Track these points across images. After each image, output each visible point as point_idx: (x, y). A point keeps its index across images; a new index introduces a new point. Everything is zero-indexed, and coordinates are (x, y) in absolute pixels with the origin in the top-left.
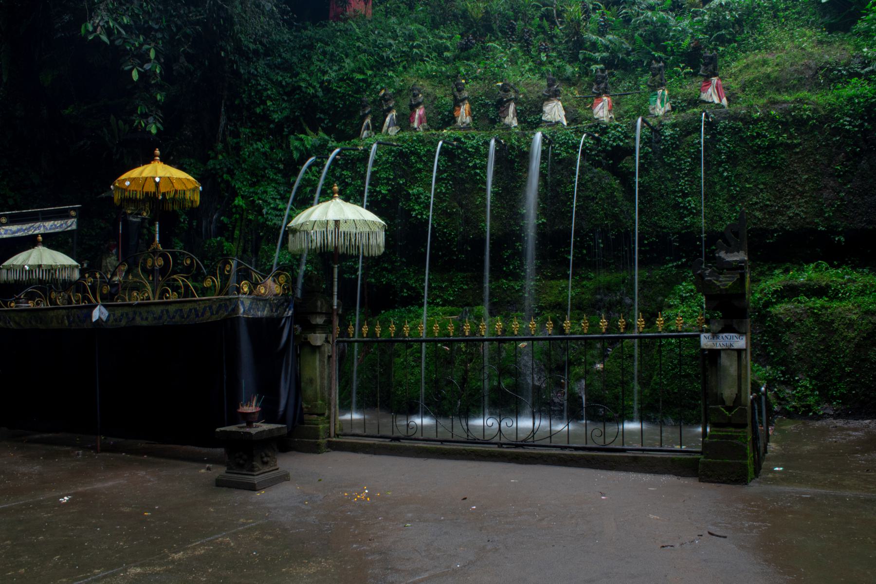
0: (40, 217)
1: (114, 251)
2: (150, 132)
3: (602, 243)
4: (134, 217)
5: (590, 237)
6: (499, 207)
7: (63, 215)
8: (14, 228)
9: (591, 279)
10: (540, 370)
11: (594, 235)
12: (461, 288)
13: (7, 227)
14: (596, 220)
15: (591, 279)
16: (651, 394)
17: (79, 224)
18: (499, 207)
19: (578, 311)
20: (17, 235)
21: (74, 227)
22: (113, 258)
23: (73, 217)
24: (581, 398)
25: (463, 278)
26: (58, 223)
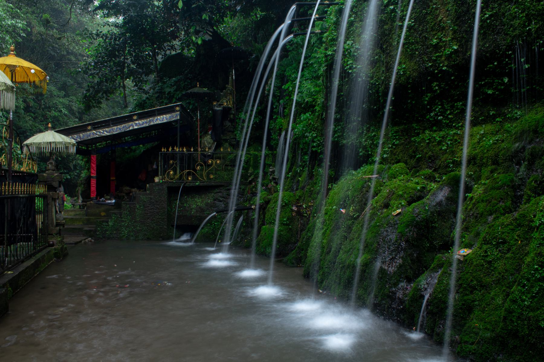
0: (156, 113)
1: (210, 132)
2: (197, 43)
3: (527, 62)
4: (217, 107)
5: (509, 56)
6: (412, 44)
7: (170, 110)
8: (140, 122)
9: (517, 119)
10: (398, 249)
11: (514, 53)
12: (394, 144)
13: (137, 122)
14: (515, 29)
15: (517, 119)
16: (505, 318)
17: (181, 115)
18: (412, 44)
19: (493, 167)
20: (142, 126)
21: (178, 118)
22: (208, 137)
23: (177, 111)
24: (423, 297)
25: (396, 132)
26: (168, 116)
